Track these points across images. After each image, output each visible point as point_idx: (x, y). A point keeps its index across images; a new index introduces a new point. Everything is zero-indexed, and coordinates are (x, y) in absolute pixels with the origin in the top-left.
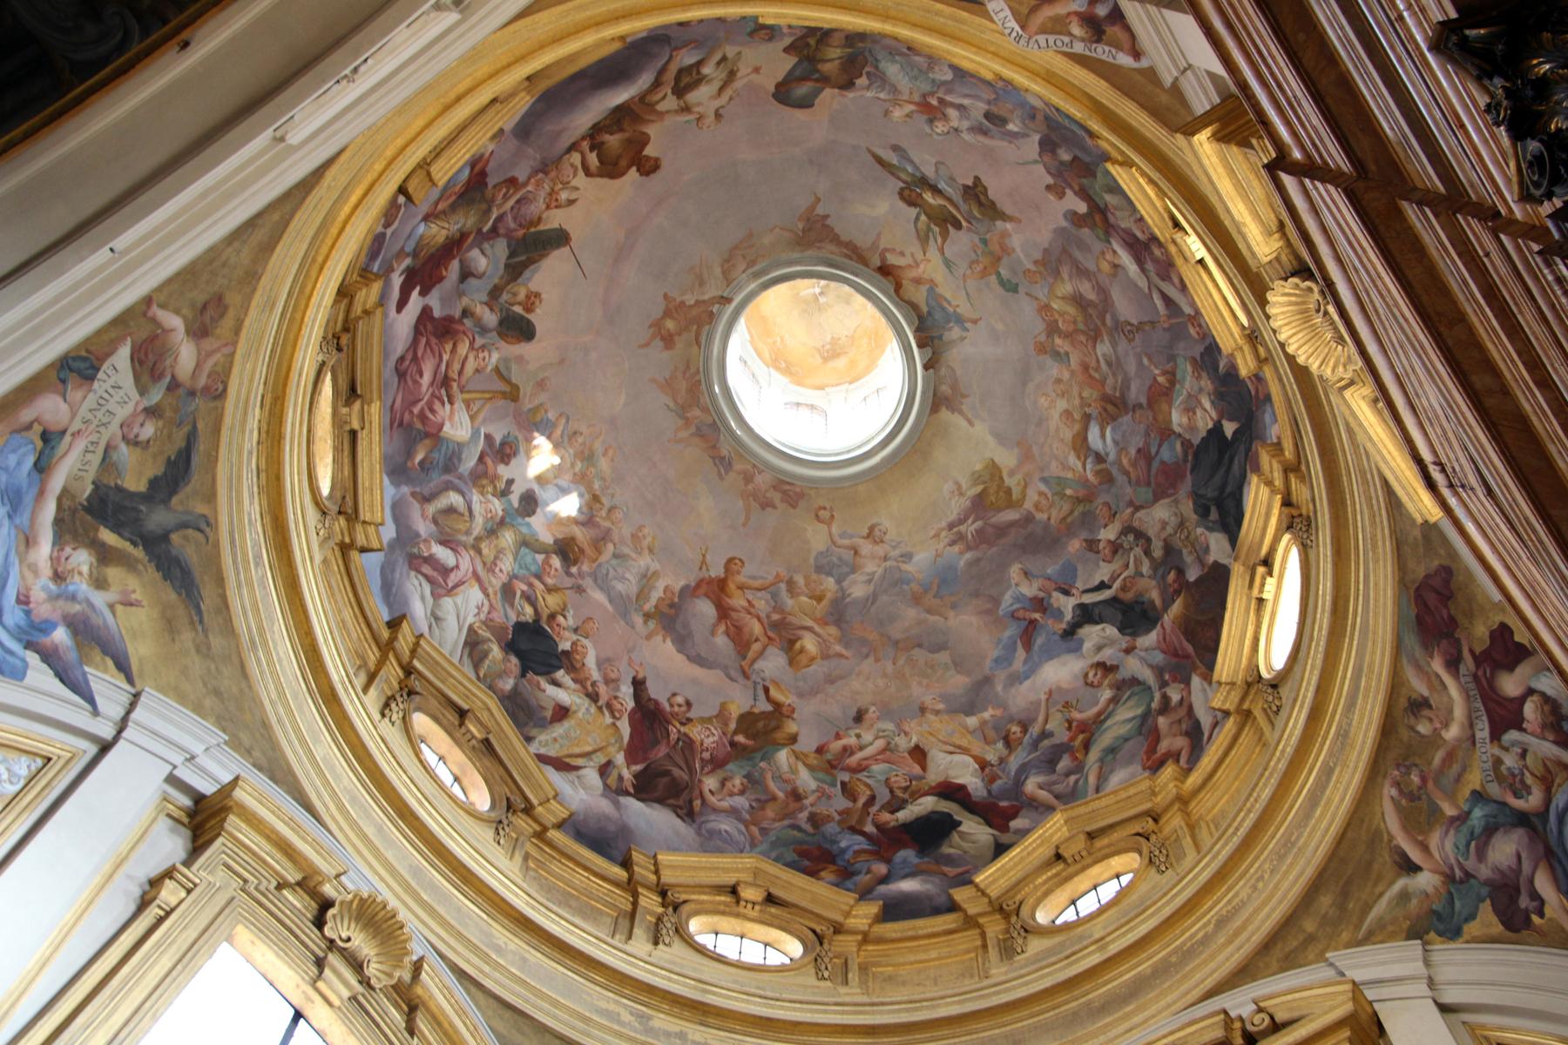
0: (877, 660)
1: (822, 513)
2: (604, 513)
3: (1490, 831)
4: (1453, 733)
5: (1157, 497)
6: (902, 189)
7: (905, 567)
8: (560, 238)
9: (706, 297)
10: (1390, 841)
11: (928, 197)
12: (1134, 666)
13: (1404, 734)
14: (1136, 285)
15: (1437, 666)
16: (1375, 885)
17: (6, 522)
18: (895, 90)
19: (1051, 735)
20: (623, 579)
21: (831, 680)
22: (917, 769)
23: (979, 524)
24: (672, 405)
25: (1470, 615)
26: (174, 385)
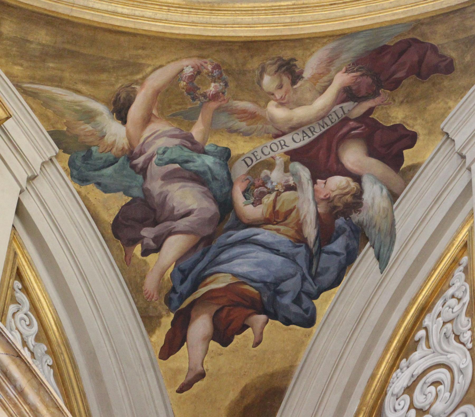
3: (198, 178)
4: (277, 112)
10: (137, 82)
13: (254, 64)
15: (341, 79)
16: (86, 82)
25: (409, 100)
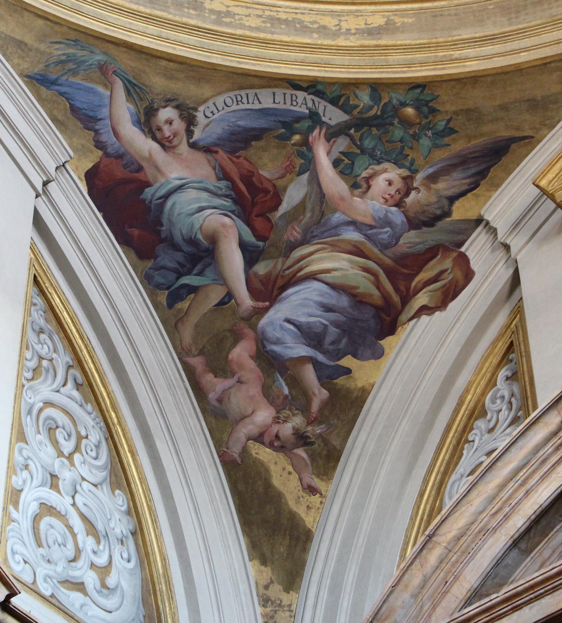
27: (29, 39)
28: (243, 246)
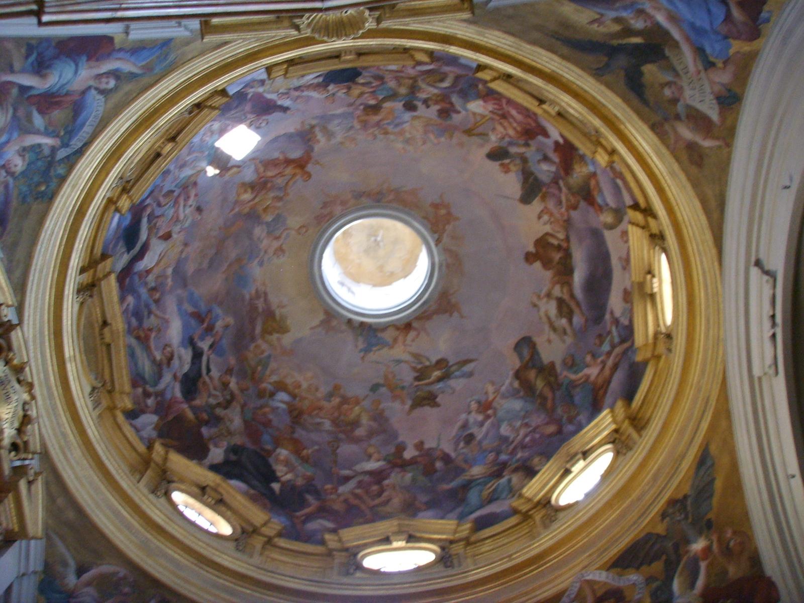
0: (220, 228)
1: (304, 230)
2: (376, 132)
5: (246, 422)
6: (448, 362)
7: (256, 262)
8: (526, 198)
9: (445, 235)
11: (437, 373)
12: (167, 378)
14: (357, 463)
17: (692, 20)
18: (504, 397)
19: (149, 317)
20: (339, 125)
21: (225, 200)
22: (161, 233)
23: (260, 310)
24: (404, 189)
26: (678, 117)
27: (186, 48)
28: (30, 88)
